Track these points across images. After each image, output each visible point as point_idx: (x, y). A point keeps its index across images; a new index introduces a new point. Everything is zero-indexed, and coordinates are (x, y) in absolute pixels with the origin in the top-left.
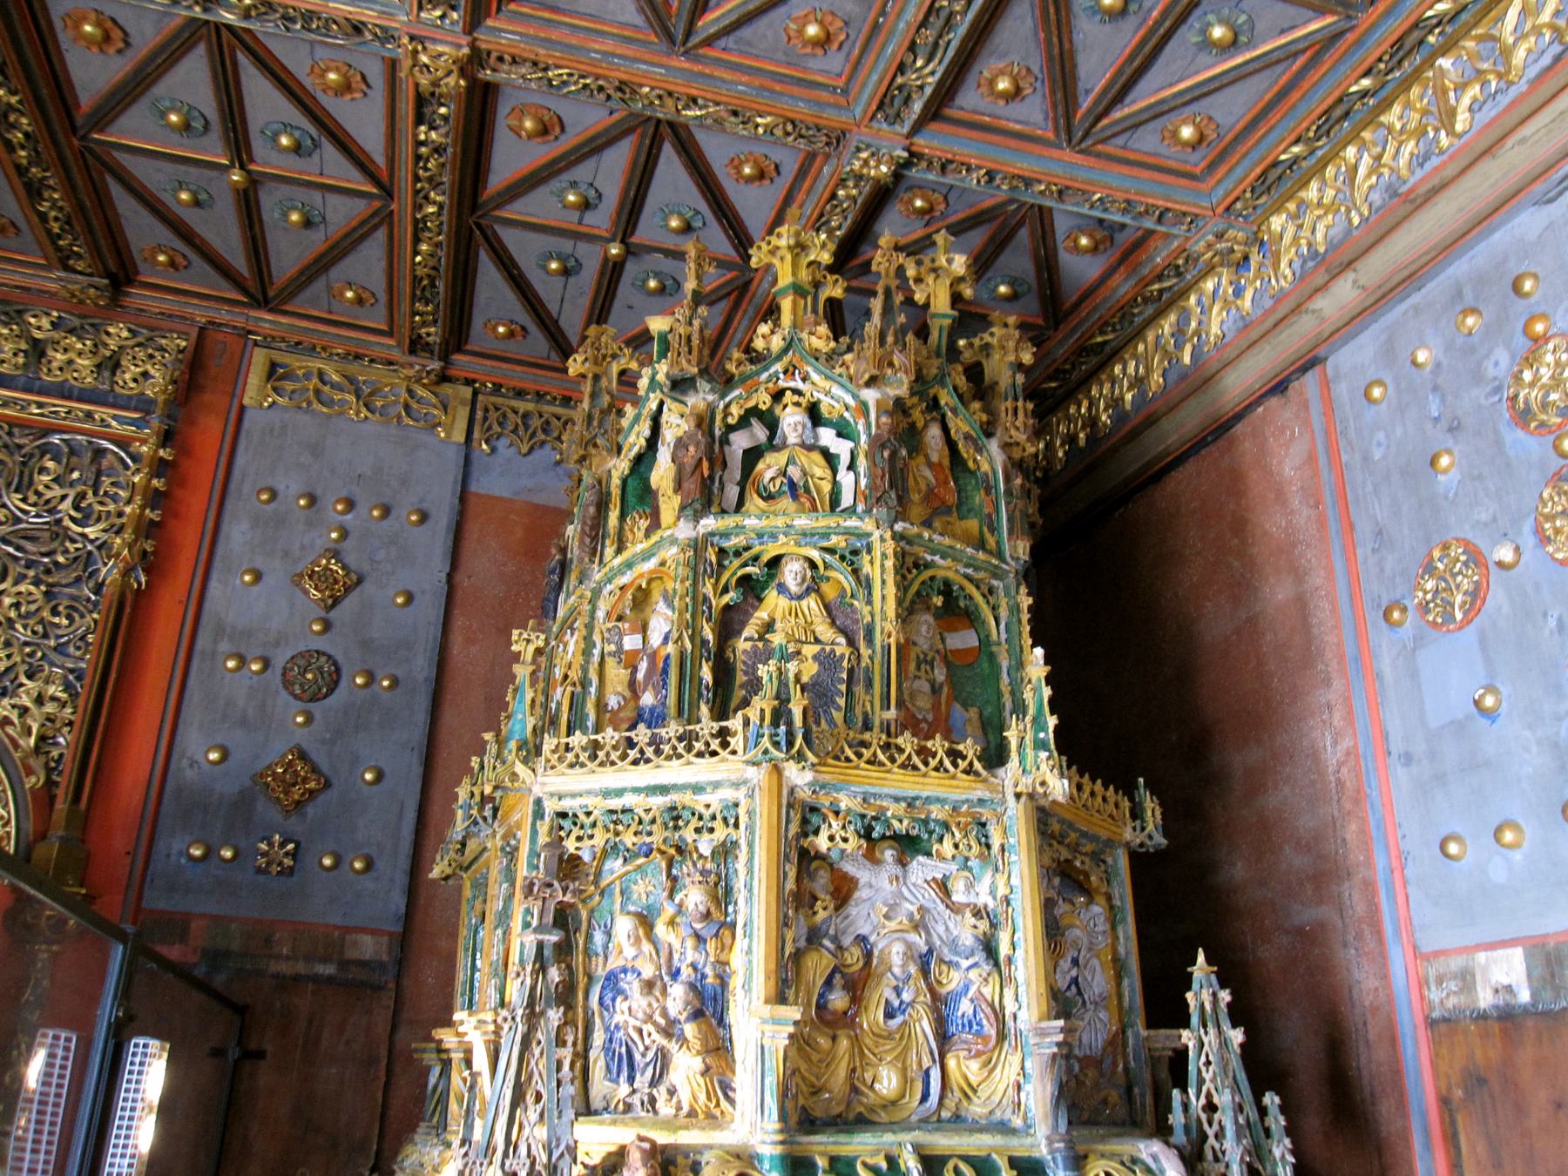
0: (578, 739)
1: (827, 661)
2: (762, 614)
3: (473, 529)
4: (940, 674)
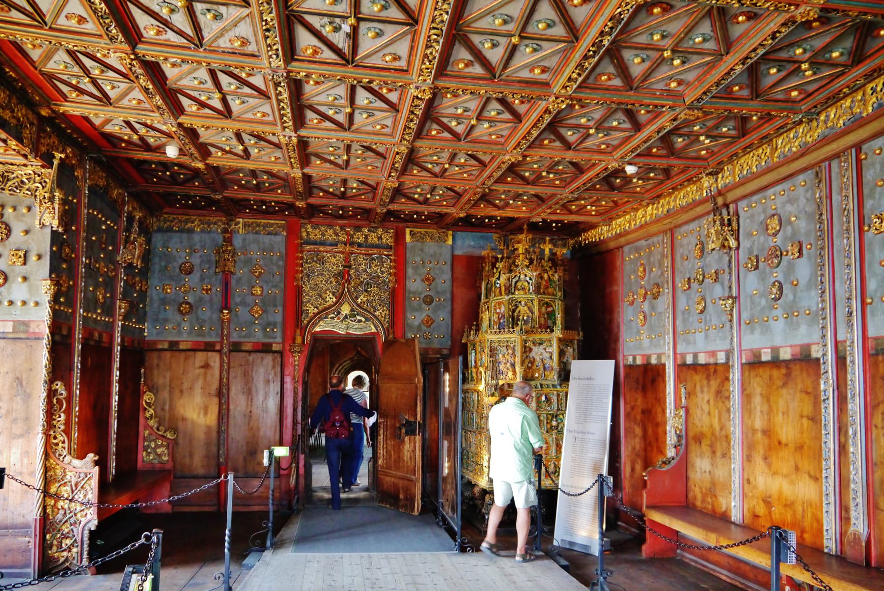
0: (493, 331)
1: (528, 317)
2: (518, 310)
3: (455, 264)
4: (546, 316)
